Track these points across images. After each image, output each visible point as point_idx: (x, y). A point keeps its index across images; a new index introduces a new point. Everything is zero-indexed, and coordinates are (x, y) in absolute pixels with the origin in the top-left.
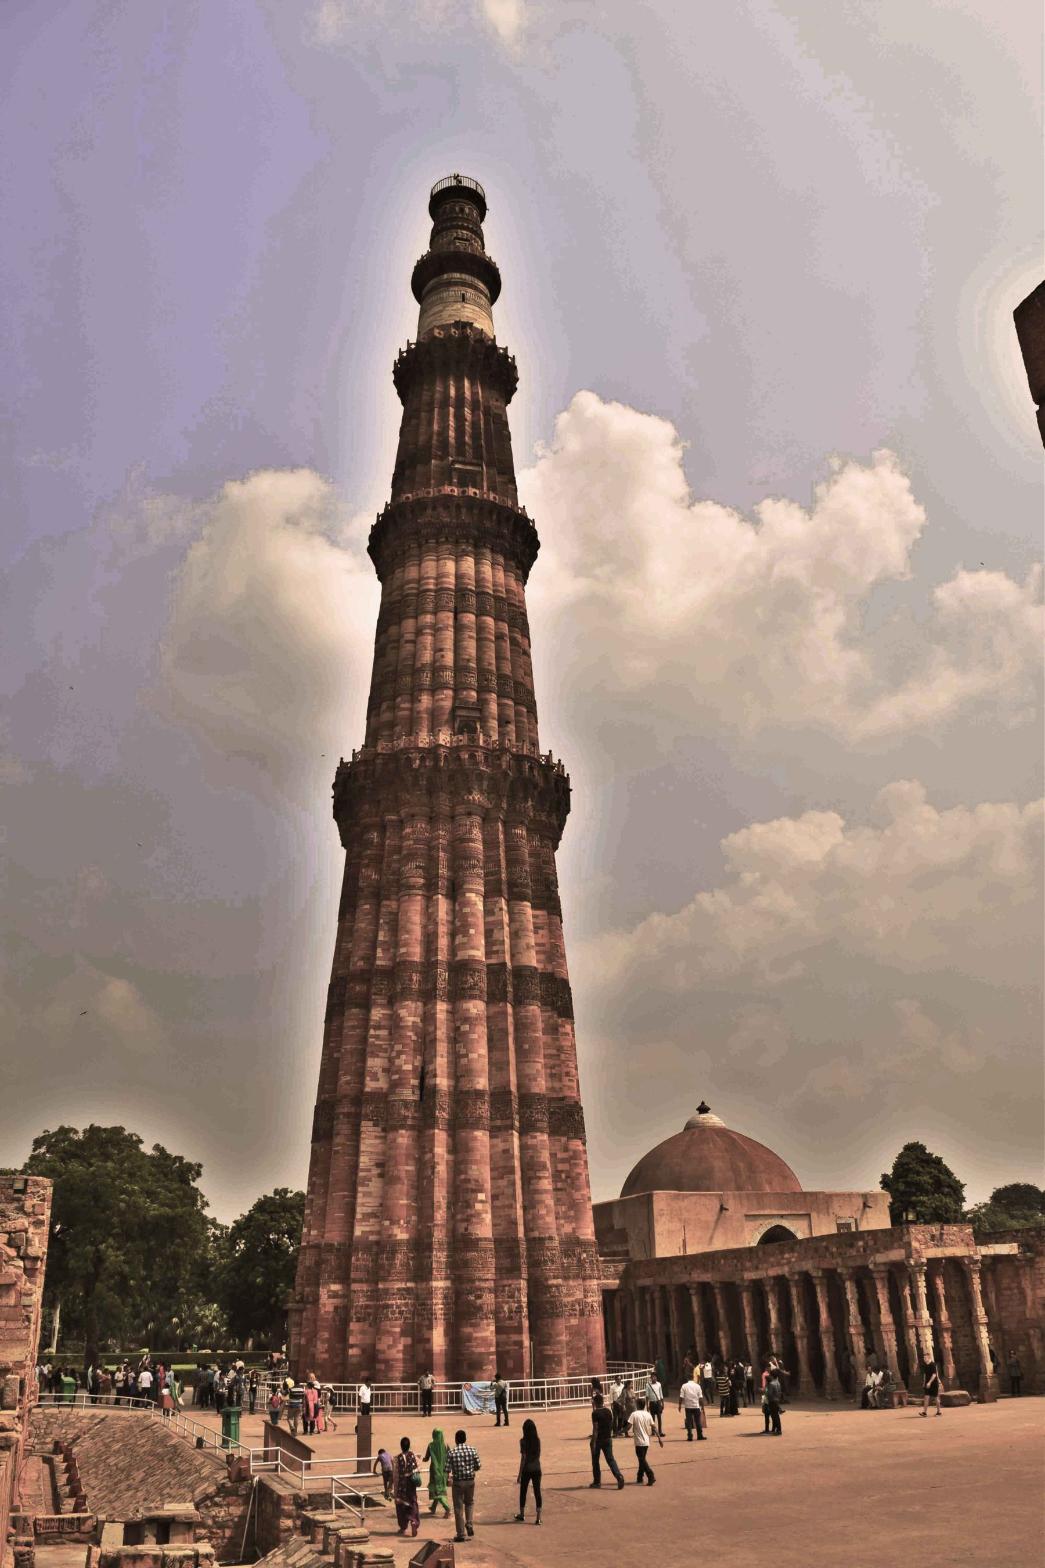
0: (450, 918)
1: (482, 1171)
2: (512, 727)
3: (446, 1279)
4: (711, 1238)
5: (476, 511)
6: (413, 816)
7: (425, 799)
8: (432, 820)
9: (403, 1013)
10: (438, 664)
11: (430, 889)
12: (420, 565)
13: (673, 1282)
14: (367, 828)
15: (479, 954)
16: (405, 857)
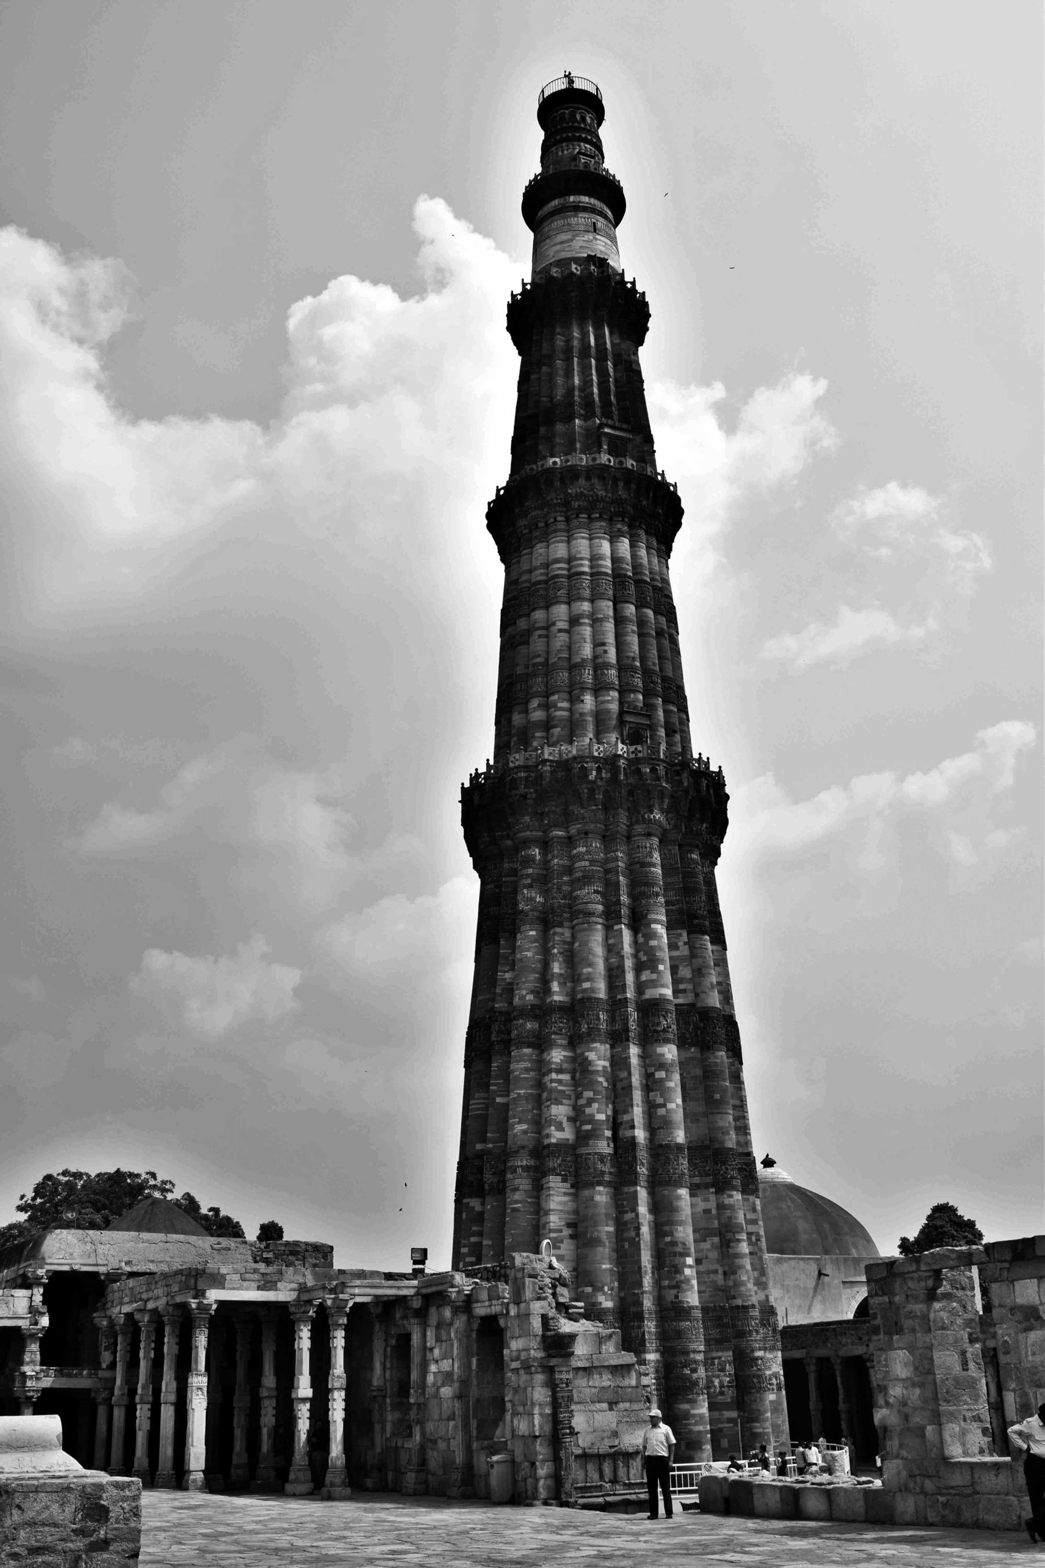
0: (633, 951)
1: (685, 1233)
2: (678, 737)
3: (656, 1351)
4: (810, 1306)
5: (633, 486)
6: (586, 833)
7: (600, 815)
8: (608, 839)
9: (592, 1056)
10: (600, 660)
11: (611, 916)
12: (568, 542)
13: (840, 1354)
14: (526, 843)
15: (668, 992)
16: (579, 879)
